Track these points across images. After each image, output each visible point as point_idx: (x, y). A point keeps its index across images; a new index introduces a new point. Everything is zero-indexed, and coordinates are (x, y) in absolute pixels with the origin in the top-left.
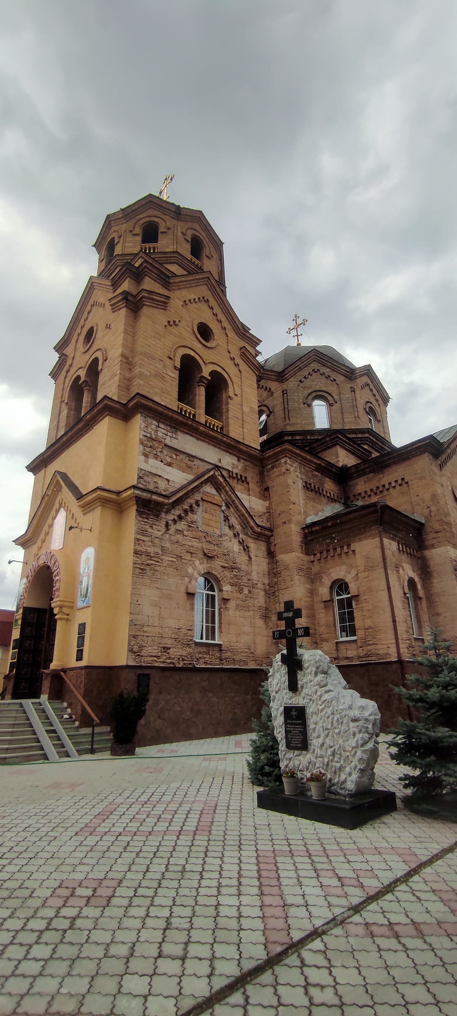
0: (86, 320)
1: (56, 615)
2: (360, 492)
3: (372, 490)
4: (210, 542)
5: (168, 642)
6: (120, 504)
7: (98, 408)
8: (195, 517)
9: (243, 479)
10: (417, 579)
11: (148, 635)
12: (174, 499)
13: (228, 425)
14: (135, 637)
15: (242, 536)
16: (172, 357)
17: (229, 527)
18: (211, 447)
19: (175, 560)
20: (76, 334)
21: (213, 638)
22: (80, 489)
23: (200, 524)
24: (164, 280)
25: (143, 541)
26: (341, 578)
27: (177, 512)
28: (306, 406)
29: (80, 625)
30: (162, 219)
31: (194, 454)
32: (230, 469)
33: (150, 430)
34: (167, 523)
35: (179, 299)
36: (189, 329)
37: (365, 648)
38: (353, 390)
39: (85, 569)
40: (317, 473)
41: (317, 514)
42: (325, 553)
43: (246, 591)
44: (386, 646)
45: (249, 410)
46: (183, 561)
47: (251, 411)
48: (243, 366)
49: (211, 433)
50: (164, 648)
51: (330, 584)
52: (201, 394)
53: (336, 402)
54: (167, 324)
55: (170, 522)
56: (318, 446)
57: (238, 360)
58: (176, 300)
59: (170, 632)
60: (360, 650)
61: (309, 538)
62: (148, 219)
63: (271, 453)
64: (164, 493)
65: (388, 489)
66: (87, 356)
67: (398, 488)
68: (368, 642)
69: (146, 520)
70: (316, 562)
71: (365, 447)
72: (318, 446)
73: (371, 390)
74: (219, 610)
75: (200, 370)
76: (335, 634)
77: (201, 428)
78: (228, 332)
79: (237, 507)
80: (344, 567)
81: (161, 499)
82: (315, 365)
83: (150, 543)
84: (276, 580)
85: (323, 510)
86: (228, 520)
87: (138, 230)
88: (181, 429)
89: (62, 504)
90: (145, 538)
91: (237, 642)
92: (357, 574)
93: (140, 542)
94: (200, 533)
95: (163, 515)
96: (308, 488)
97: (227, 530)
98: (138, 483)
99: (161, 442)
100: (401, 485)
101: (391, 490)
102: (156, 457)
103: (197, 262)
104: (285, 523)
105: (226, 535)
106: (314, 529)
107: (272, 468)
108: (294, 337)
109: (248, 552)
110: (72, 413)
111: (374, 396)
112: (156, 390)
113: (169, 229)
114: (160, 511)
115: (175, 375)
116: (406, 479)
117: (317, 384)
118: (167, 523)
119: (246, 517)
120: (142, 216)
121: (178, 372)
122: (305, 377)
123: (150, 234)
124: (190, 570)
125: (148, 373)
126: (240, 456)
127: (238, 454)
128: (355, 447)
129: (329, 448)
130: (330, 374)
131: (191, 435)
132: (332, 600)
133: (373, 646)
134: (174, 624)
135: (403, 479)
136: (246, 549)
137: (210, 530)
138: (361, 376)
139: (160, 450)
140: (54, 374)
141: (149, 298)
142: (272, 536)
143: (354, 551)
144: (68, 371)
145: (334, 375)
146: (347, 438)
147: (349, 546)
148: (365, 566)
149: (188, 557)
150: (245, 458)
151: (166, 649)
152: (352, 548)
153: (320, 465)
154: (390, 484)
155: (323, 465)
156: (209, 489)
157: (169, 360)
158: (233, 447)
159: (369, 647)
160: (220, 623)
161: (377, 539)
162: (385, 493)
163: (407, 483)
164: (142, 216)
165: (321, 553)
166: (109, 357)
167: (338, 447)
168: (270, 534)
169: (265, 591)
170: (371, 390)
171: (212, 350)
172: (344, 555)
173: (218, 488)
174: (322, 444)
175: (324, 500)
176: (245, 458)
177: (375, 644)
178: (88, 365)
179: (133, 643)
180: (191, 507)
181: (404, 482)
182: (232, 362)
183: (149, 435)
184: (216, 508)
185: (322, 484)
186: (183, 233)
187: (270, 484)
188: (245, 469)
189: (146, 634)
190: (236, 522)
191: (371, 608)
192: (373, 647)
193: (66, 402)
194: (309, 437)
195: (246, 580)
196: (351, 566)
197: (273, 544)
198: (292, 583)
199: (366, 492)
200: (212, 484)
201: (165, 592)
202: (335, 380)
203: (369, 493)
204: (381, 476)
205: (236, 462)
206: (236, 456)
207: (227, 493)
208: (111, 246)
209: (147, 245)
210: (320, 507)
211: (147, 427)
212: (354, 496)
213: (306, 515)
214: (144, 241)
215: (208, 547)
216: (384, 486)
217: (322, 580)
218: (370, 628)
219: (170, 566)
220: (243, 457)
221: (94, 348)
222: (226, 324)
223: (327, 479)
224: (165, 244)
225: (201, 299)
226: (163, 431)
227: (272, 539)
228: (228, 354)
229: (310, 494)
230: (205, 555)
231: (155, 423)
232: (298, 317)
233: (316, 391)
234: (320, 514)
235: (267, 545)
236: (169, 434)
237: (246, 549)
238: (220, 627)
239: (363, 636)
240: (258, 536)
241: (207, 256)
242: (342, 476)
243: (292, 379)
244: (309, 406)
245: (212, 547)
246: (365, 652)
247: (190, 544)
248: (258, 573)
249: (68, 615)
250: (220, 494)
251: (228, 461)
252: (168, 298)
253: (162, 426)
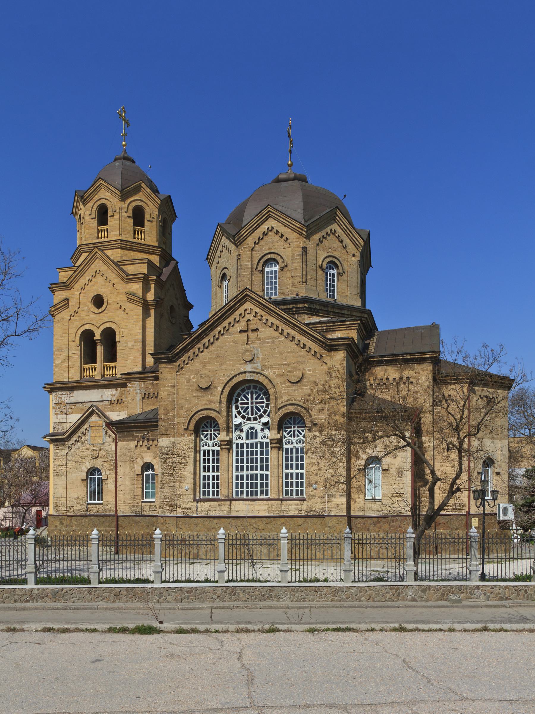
5: (73, 504)
8: (87, 437)
45: (133, 342)
47: (135, 342)
94: (89, 446)
134: (76, 495)
151: (72, 507)
183: (57, 402)
236: (69, 396)
253: (64, 393)
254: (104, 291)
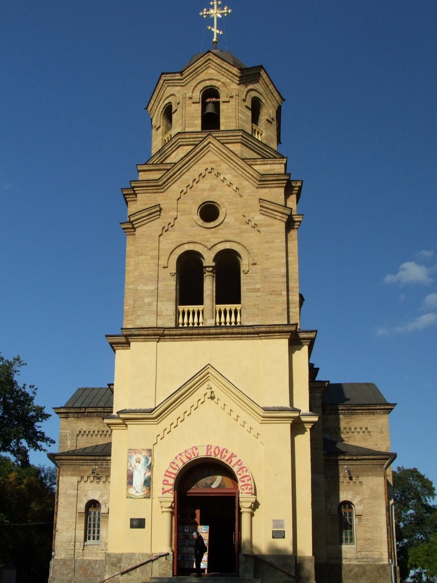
37: (363, 553)
44: (380, 553)
60: (359, 554)
80: (351, 493)
92: (362, 500)
152: (360, 479)
159: (367, 553)
177: (372, 551)
191: (371, 526)
192: (370, 553)
196: (357, 493)
218: (369, 539)
221: (222, 233)
246: (362, 556)
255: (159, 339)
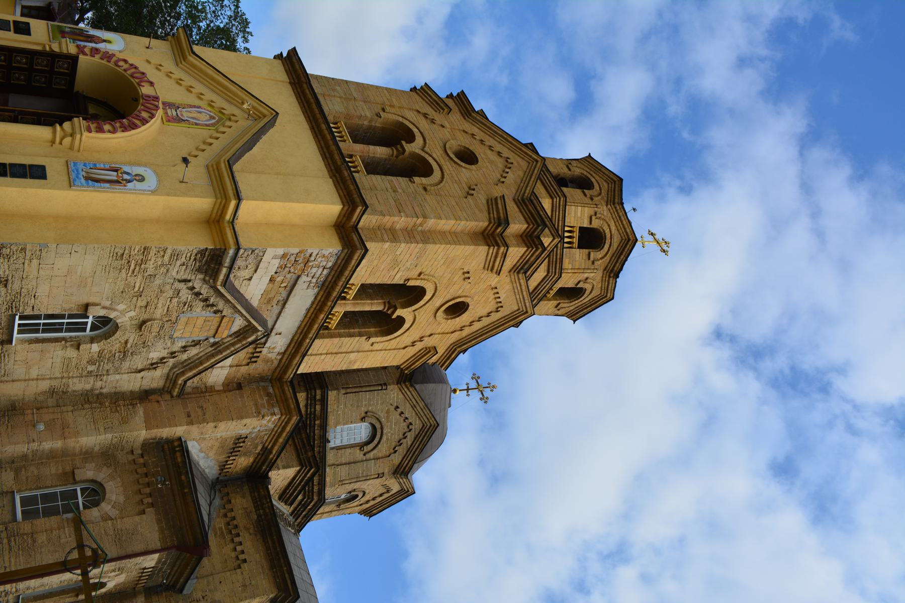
0: (490, 147)
1: (61, 125)
2: (233, 501)
3: (234, 518)
4: (162, 327)
6: (218, 222)
7: (354, 192)
8: (199, 310)
9: (253, 360)
10: (103, 590)
11: (26, 264)
12: (223, 290)
13: (331, 336)
14: (23, 250)
15: (172, 361)
16: (422, 276)
17: (184, 347)
18: (297, 324)
19: (136, 289)
20: (475, 130)
21: (19, 332)
22: (248, 154)
23: (189, 315)
24: (522, 268)
25: (163, 256)
26: (107, 496)
27: (205, 291)
28: (363, 415)
29: (42, 168)
30: (607, 253)
31: (287, 306)
32: (267, 345)
33: (319, 260)
34: (190, 281)
35: (499, 282)
36: (460, 293)
38: (380, 476)
39: (128, 174)
40: (260, 448)
41: (201, 451)
42: (145, 470)
43: (91, 368)
46: (135, 298)
47: (350, 362)
48: (411, 351)
49: (316, 326)
50: (7, 281)
51: (99, 480)
52: (376, 306)
53: (364, 455)
54: (465, 270)
55: (190, 284)
56: (303, 442)
57: (419, 346)
58: (497, 279)
59: (30, 287)
61: (166, 447)
62: (608, 236)
63: (287, 392)
64: (232, 276)
65: (232, 541)
66: (438, 153)
67: (233, 555)
68: (12, 539)
69: (193, 258)
70: (131, 457)
71: (300, 497)
72: (303, 442)
73: (381, 495)
74: (64, 339)
75: (404, 307)
76: (26, 490)
77: (322, 316)
78: (457, 333)
79: (213, 356)
80: (122, 499)
81: (221, 277)
82: (417, 425)
83: (160, 263)
84: (107, 404)
85: (208, 457)
86: (195, 345)
87: (596, 224)
88: (322, 293)
89: (230, 120)
90: (166, 258)
91: (15, 361)
93: (162, 253)
94: (175, 314)
95: (201, 276)
96: (238, 439)
97: (180, 344)
98: (245, 250)
99: (303, 271)
100: (237, 558)
101: (231, 546)
102: (282, 267)
103: (552, 293)
104: (189, 416)
105: (173, 343)
106: (178, 454)
107: (268, 395)
108: (467, 384)
109: (149, 369)
110: (366, 123)
111: (374, 499)
112: (376, 262)
113: (593, 263)
114: (206, 273)
115: (398, 280)
116: (245, 566)
117: (391, 429)
118: (190, 281)
119: (198, 365)
120: (613, 228)
121: (402, 282)
122: (402, 413)
123: (590, 239)
124: (121, 307)
125: (398, 253)
126: (286, 356)
127: (288, 353)
128: (297, 487)
129: (298, 456)
130: (404, 445)
131: (313, 303)
132: (75, 482)
133: (7, 547)
135: (245, 561)
136: (153, 366)
137: (180, 326)
138: (400, 483)
139: (292, 270)
140: (425, 92)
141: (497, 253)
142: (172, 397)
143: (143, 512)
144: (425, 115)
145: (402, 450)
146: (311, 478)
147: (152, 505)
148: (122, 530)
149: (142, 302)
150: (284, 361)
153: (271, 452)
154: (240, 544)
155: (271, 456)
156: (239, 323)
157: (418, 273)
158: (299, 346)
159: (5, 541)
160: (44, 341)
161: (158, 545)
162: (228, 537)
163: (239, 567)
164: (613, 228)
165: (145, 465)
166: (427, 197)
167: (298, 468)
168: (175, 394)
169: (92, 390)
170: (381, 495)
171: (432, 317)
172: (139, 497)
173: (241, 334)
174: (304, 446)
175: (222, 458)
176: (284, 361)
177: (10, 550)
178: (426, 156)
179: (14, 248)
180: (213, 305)
181: (240, 563)
182: (417, 338)
183: (312, 258)
184: (212, 332)
185: (245, 454)
186: (587, 279)
187: (246, 391)
188: (267, 361)
189: (27, 262)
190: (192, 354)
193: (382, 114)
194: (317, 422)
195: (106, 367)
197: (159, 399)
198: (102, 429)
199: (232, 510)
200: (246, 326)
201: (89, 280)
202: (395, 452)
203: (229, 514)
204: (251, 531)
205: (277, 350)
206: (285, 351)
207: (233, 344)
208: (583, 184)
209: (576, 234)
210: (211, 454)
211: (324, 256)
212: (228, 493)
213: (200, 440)
214: (582, 229)
215: (155, 325)
216: (238, 535)
217: (105, 468)
218: (34, 541)
219: (127, 285)
220: (285, 358)
221: (448, 166)
222: (467, 331)
223: (252, 460)
224: (575, 258)
225: (500, 305)
226: (319, 272)
227: (167, 397)
228: (428, 334)
229: (230, 444)
230: (144, 322)
231: (330, 264)
232: (492, 391)
233: (382, 428)
234: (203, 454)
235: (159, 390)
236: (314, 280)
237: (153, 366)
238: (37, 341)
239: (22, 531)
240: (171, 380)
241: (559, 304)
242: (256, 477)
243: (401, 396)
244: (363, 419)
245: (155, 329)
247: (160, 305)
248: (117, 381)
249: (61, 143)
250: (231, 336)
251: (277, 343)
252: (498, 273)
253: (325, 272)
254: (465, 318)
255: (294, 84)
